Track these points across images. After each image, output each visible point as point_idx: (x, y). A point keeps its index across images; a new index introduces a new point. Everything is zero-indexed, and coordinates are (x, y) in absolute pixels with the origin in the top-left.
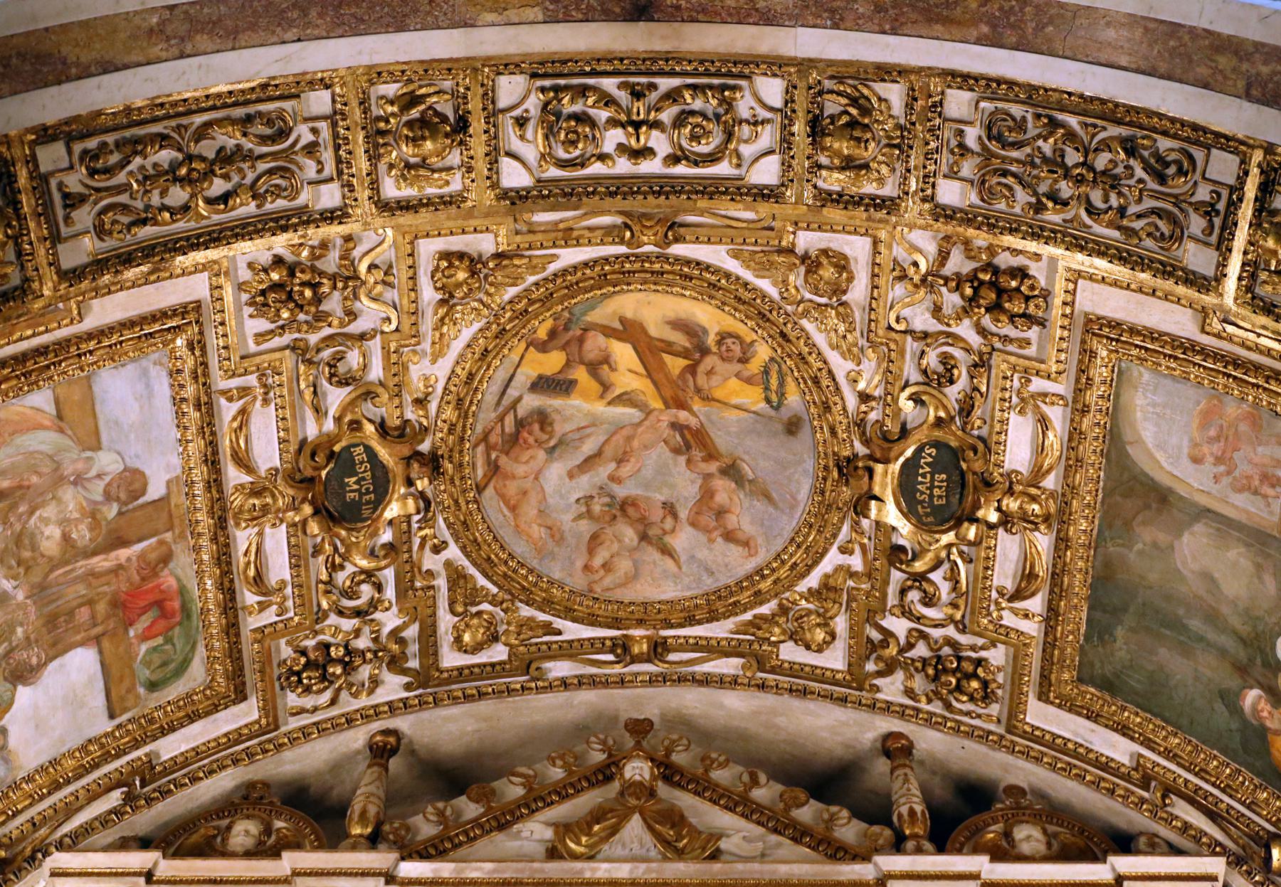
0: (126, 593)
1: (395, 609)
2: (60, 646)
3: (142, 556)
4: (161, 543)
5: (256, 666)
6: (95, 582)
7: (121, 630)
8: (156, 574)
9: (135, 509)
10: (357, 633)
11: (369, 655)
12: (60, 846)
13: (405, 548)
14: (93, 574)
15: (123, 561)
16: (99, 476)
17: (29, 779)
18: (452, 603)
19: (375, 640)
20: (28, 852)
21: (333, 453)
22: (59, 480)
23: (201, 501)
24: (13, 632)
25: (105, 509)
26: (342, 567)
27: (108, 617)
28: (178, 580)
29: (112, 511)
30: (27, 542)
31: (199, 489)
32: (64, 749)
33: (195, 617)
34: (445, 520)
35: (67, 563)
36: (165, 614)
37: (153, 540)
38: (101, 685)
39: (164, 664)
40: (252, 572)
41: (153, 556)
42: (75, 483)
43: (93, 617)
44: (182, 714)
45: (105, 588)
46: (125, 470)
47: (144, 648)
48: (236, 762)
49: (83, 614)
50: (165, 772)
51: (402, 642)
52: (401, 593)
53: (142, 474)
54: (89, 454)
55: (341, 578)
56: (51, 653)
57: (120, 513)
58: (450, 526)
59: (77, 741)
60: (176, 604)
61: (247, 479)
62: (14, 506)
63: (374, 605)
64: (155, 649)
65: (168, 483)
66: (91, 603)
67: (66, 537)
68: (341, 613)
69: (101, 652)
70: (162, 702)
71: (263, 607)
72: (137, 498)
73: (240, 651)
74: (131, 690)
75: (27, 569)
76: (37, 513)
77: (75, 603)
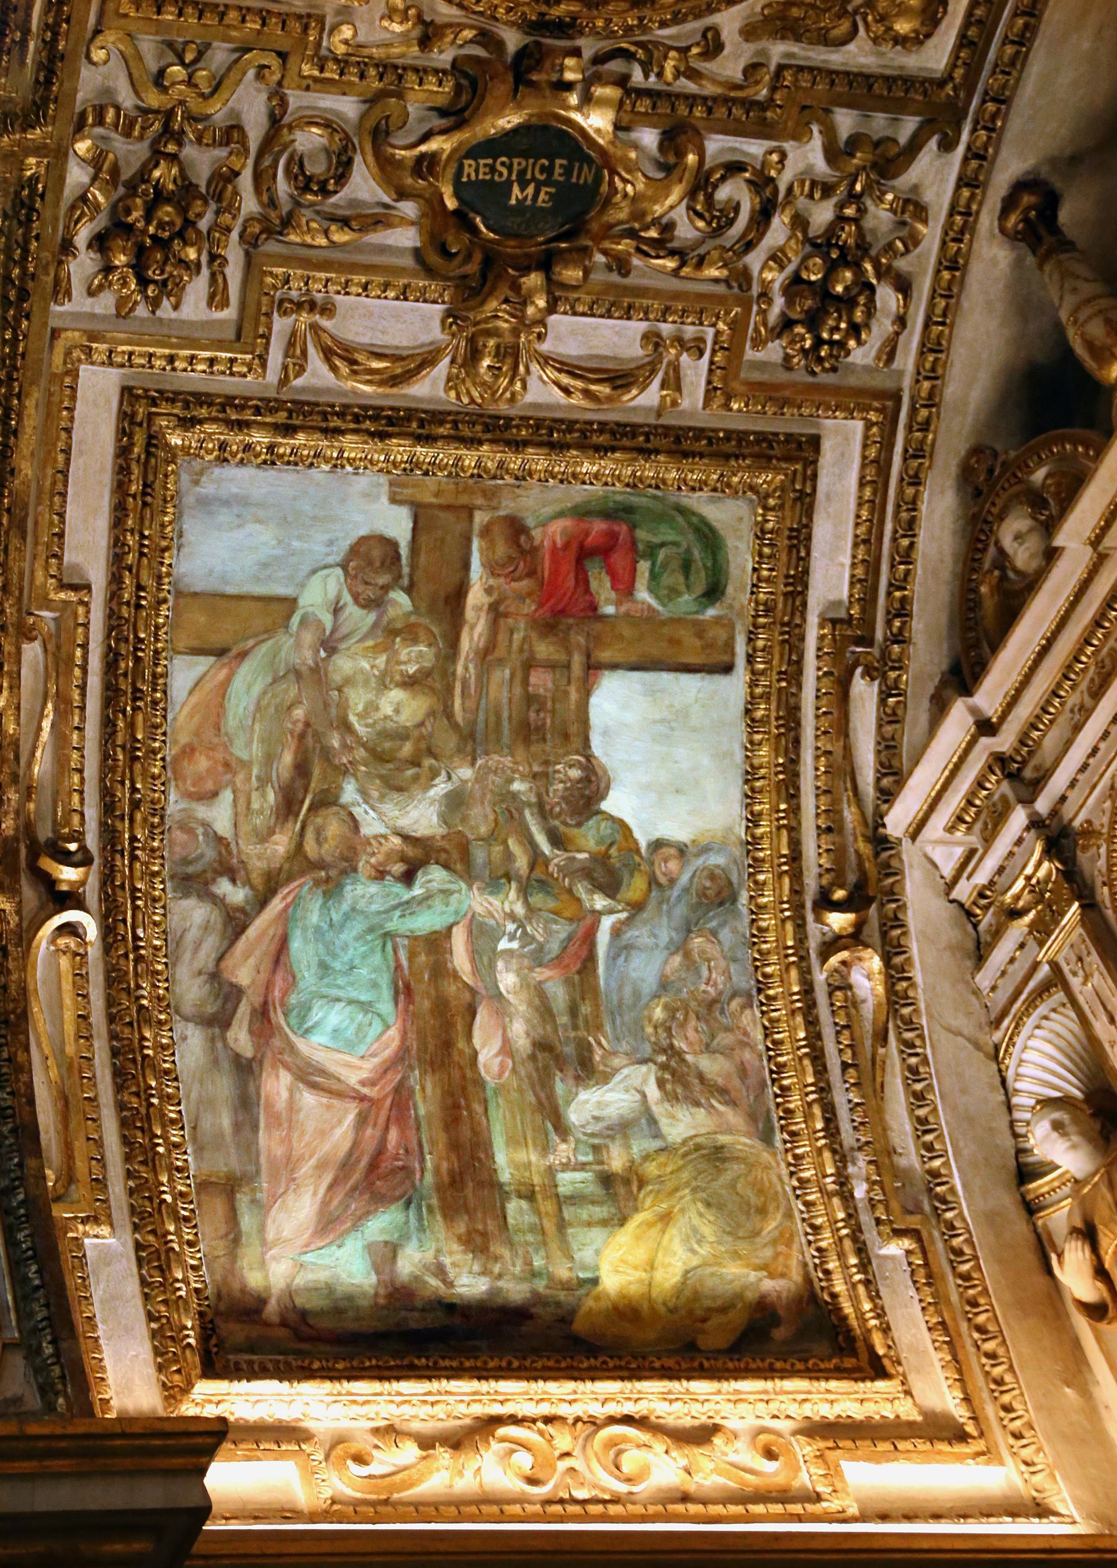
0: (541, 605)
1: (788, 146)
2: (573, 729)
3: (492, 567)
4: (486, 532)
5: (770, 409)
6: (500, 652)
7: (598, 626)
8: (534, 550)
9: (413, 566)
10: (800, 222)
11: (850, 211)
12: (887, 796)
13: (683, 110)
14: (486, 655)
15: (486, 600)
16: (337, 611)
17: (754, 820)
18: (825, 40)
19: (828, 190)
20: (865, 848)
21: (456, 212)
22: (317, 675)
23: (445, 454)
24: (514, 796)
25: (391, 612)
26: (668, 228)
27: (566, 646)
28: (561, 514)
29: (400, 599)
30: (388, 745)
31: (423, 452)
32: (739, 755)
33: (635, 500)
34: (663, 24)
35: (449, 690)
36: (605, 550)
37: (476, 544)
38: (666, 677)
39: (686, 567)
40: (603, 390)
41: (502, 549)
42: (332, 651)
43: (551, 666)
44: (784, 557)
45: (517, 637)
46: (344, 566)
47: (643, 594)
48: (916, 481)
49: (540, 681)
50: (868, 601)
51: (855, 141)
52: (763, 131)
53: (363, 540)
54: (295, 620)
55: (687, 230)
56: (576, 743)
57: (409, 590)
58: (678, 19)
59: (738, 733)
60: (599, 526)
61: (443, 367)
62: (326, 754)
63: (762, 183)
64: (654, 576)
65: (394, 500)
66: (529, 665)
67: (410, 683)
68: (749, 246)
69: (614, 667)
70: (749, 579)
71: (674, 382)
72: (397, 557)
73: (729, 434)
74: (700, 630)
75: (431, 753)
76: (353, 719)
77: (518, 690)
